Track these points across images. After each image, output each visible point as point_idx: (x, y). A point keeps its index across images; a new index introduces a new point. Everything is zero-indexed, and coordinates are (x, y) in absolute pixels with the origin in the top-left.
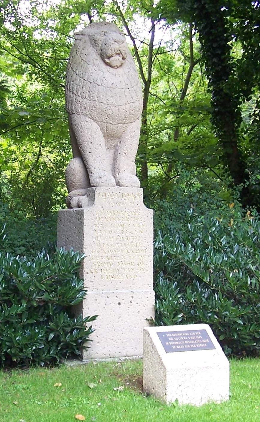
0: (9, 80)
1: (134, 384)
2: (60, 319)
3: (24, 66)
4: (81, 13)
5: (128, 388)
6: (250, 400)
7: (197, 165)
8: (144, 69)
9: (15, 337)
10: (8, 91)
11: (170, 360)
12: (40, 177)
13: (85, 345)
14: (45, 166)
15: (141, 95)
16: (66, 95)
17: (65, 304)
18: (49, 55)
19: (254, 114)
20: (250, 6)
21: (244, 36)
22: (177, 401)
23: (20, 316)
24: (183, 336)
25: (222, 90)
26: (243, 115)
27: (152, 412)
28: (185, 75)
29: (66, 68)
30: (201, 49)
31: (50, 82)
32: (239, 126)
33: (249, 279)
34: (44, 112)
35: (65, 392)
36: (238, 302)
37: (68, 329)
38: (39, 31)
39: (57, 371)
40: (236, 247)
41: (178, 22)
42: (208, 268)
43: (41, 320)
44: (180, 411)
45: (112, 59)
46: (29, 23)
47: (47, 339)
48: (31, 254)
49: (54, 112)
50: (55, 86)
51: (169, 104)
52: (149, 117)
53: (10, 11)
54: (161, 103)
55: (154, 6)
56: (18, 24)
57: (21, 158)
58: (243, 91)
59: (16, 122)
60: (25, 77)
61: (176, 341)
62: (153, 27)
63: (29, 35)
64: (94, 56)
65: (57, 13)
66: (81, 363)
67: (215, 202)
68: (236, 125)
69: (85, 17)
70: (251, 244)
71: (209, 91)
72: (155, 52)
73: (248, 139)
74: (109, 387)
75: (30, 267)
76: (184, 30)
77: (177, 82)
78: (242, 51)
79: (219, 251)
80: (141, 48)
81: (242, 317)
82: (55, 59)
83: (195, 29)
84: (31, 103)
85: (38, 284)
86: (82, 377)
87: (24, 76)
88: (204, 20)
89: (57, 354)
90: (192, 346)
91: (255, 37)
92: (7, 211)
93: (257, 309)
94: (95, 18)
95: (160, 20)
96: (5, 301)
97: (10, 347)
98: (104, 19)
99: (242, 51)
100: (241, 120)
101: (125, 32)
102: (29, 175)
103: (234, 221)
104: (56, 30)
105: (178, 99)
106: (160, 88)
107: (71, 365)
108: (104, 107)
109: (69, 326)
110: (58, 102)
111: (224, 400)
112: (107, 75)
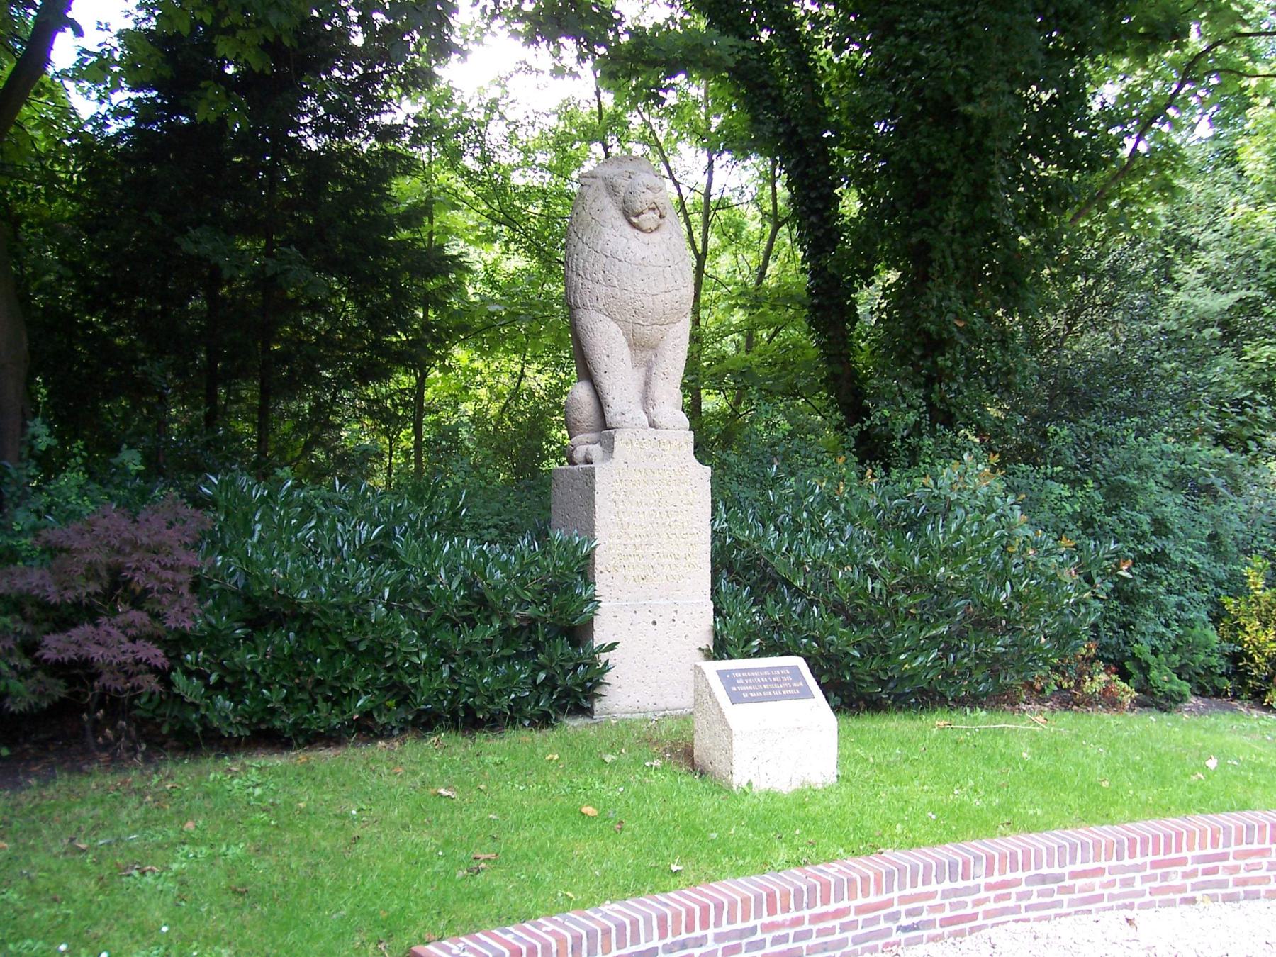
0: (471, 253)
1: (678, 757)
2: (555, 649)
3: (496, 229)
4: (590, 142)
5: (669, 763)
6: (871, 782)
7: (783, 394)
8: (696, 235)
9: (482, 678)
10: (469, 271)
11: (737, 715)
12: (523, 413)
13: (598, 691)
14: (531, 394)
15: (690, 277)
16: (565, 276)
17: (564, 623)
18: (538, 211)
19: (878, 309)
20: (871, 130)
21: (861, 179)
22: (750, 784)
23: (489, 643)
24: (760, 677)
25: (825, 268)
26: (860, 309)
27: (708, 803)
28: (764, 244)
29: (565, 233)
30: (791, 200)
31: (538, 255)
32: (853, 329)
33: (869, 582)
34: (529, 305)
35: (564, 770)
36: (851, 621)
37: (570, 666)
38: (521, 170)
39: (552, 735)
40: (848, 529)
41: (753, 156)
42: (803, 564)
43: (525, 650)
44: (756, 801)
45: (642, 217)
46: (505, 158)
47: (534, 681)
48: (507, 541)
49: (546, 306)
50: (548, 262)
51: (736, 292)
52: (704, 313)
53: (473, 137)
54: (724, 290)
55: (713, 130)
56: (485, 159)
57: (490, 381)
58: (860, 271)
59: (483, 322)
60: (497, 247)
61: (749, 684)
62: (711, 164)
63: (505, 178)
64: (612, 213)
65: (551, 142)
66: (590, 721)
67: (814, 454)
68: (849, 326)
69: (597, 148)
70: (874, 524)
71: (803, 271)
72: (713, 205)
73: (868, 350)
74: (637, 762)
75: (507, 562)
76: (761, 169)
77: (751, 256)
78: (859, 205)
79: (820, 536)
80: (692, 199)
81: (858, 645)
82: (548, 218)
83: (781, 168)
84: (508, 290)
85: (519, 590)
86: (592, 745)
87: (496, 246)
88: (795, 153)
89: (550, 707)
90: (775, 693)
91: (880, 181)
92: (469, 469)
93: (884, 631)
94: (615, 150)
95: (721, 153)
96: (464, 619)
97: (472, 695)
98: (629, 151)
99: (859, 205)
100: (857, 318)
101: (665, 172)
102: (503, 409)
103: (846, 486)
104: (549, 169)
105: (751, 284)
106: (722, 265)
107: (574, 724)
108: (629, 296)
109: (571, 659)
110: (553, 288)
111: (829, 783)
112: (634, 244)
